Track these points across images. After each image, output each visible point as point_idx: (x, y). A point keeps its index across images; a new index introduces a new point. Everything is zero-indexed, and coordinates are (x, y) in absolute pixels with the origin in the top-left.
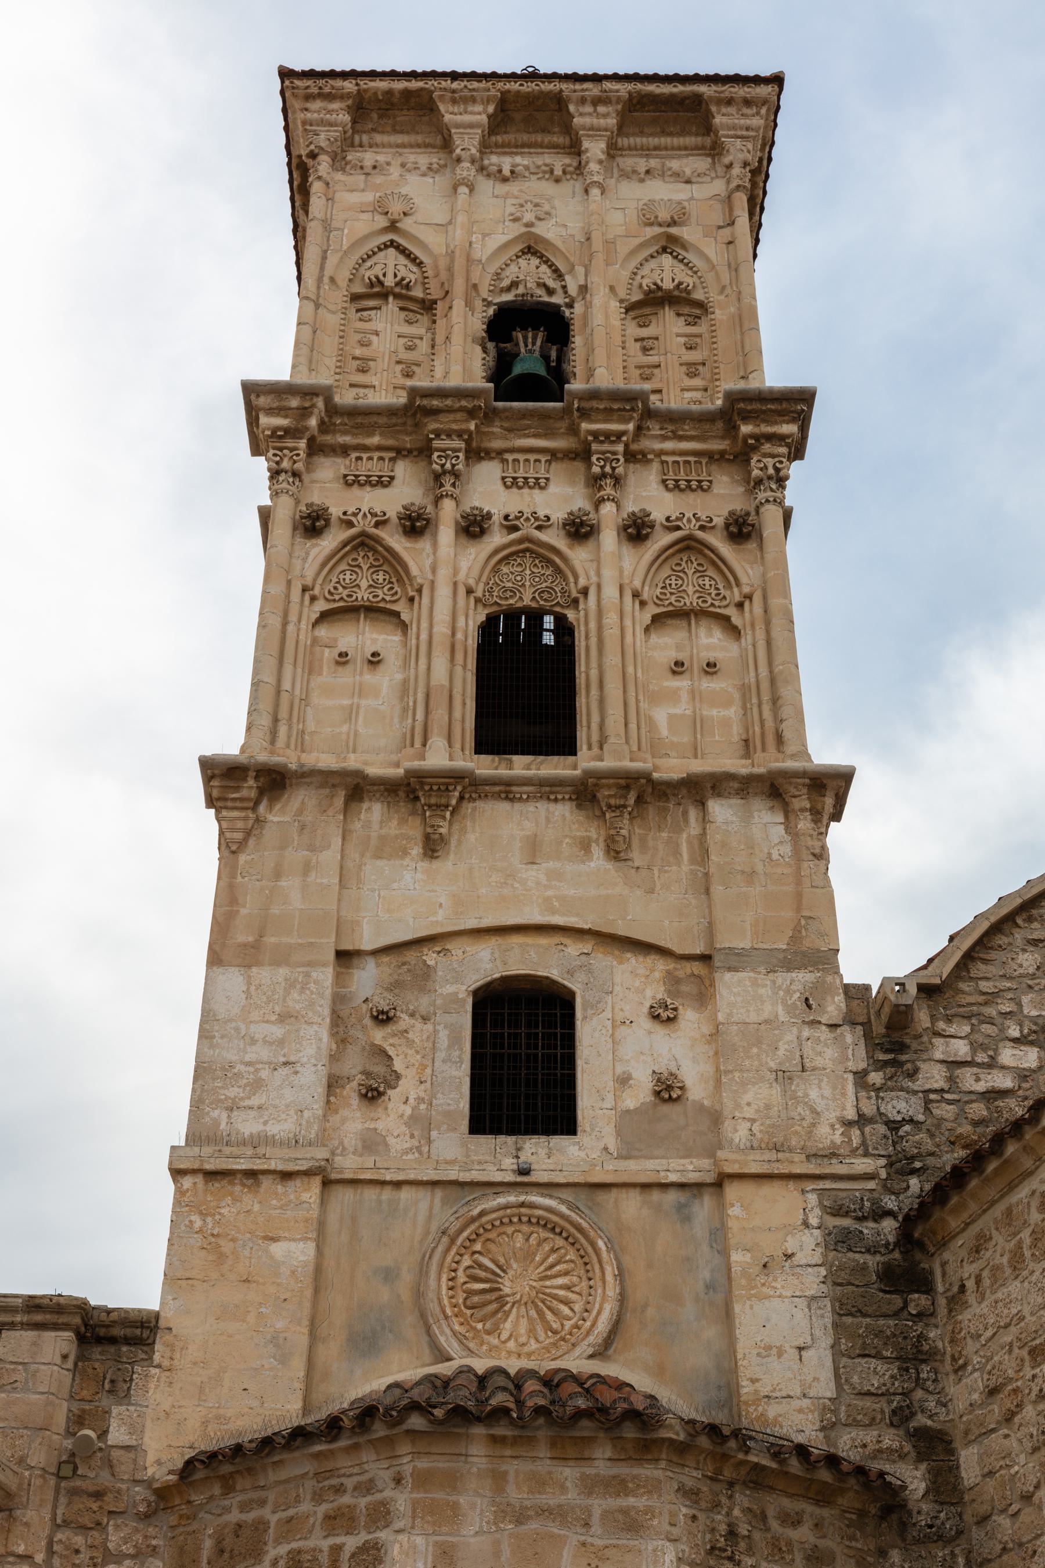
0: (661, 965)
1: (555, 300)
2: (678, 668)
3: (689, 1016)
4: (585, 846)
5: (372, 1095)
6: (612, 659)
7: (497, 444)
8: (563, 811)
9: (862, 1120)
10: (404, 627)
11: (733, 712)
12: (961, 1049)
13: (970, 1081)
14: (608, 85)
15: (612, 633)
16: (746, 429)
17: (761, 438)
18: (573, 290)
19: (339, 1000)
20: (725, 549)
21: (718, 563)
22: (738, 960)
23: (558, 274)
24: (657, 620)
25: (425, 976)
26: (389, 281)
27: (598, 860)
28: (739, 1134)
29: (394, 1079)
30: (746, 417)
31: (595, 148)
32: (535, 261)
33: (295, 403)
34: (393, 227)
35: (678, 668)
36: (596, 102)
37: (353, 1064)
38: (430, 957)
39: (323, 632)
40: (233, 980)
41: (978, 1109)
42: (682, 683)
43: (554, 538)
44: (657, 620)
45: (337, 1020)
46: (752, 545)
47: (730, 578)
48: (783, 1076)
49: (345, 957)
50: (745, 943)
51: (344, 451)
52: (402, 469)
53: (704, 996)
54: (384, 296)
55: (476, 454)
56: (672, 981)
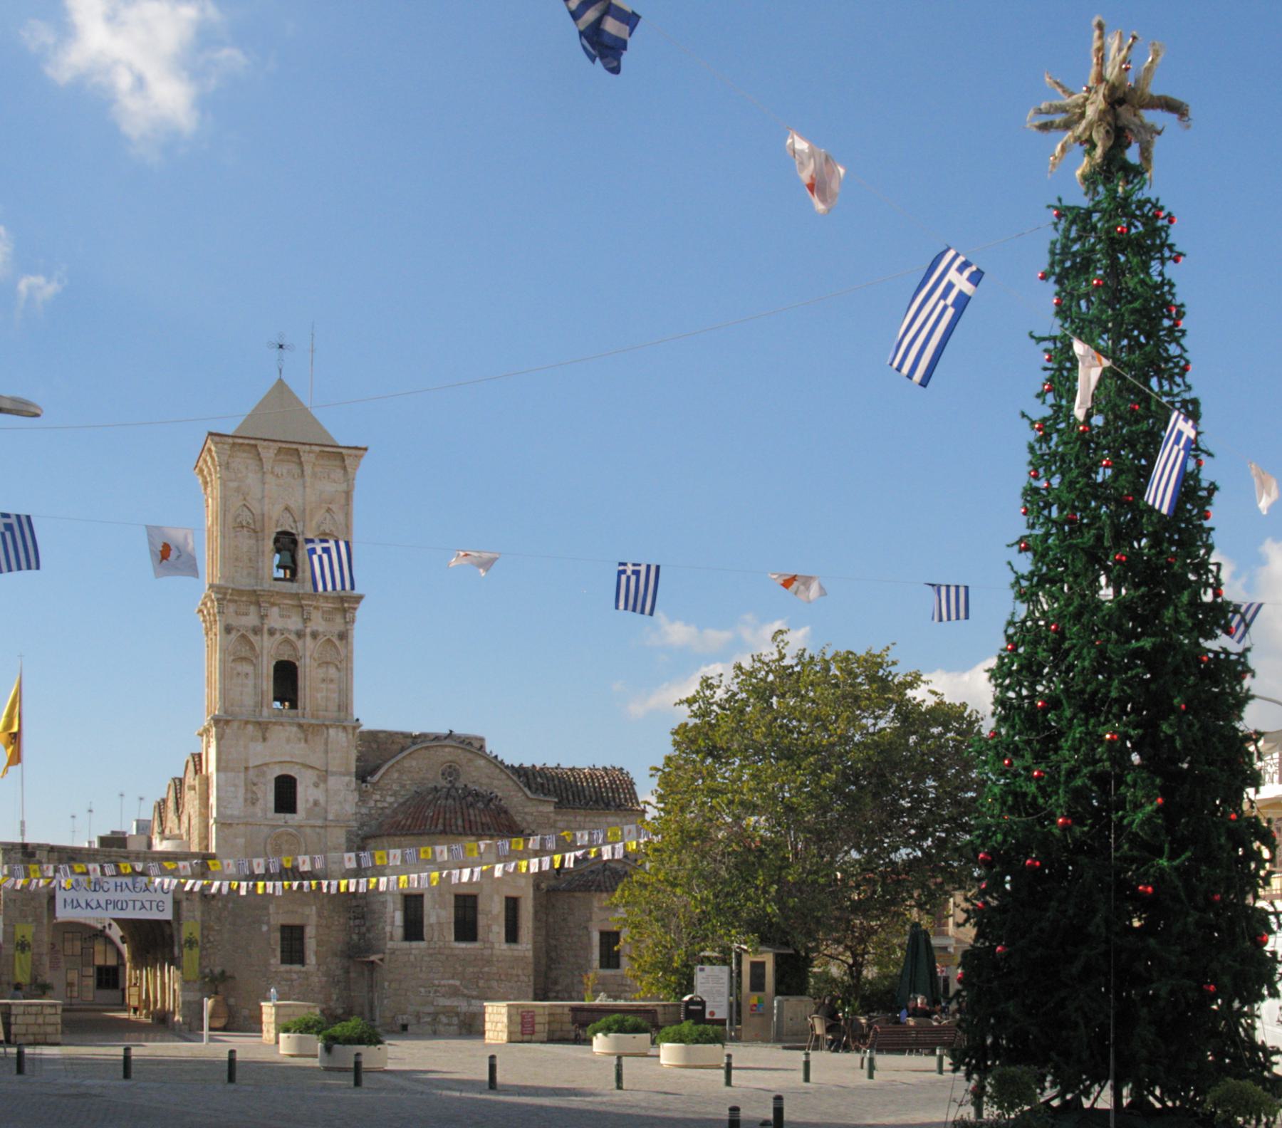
0: (317, 772)
1: (294, 531)
2: (323, 680)
3: (322, 785)
4: (300, 740)
5: (253, 804)
6: (308, 683)
7: (278, 602)
8: (295, 729)
9: (356, 814)
10: (254, 665)
11: (336, 695)
12: (378, 797)
13: (379, 805)
14: (314, 448)
15: (307, 674)
16: (346, 605)
17: (349, 608)
18: (300, 530)
19: (246, 779)
20: (337, 643)
21: (335, 646)
22: (334, 774)
23: (295, 521)
24: (319, 665)
25: (264, 773)
26: (244, 523)
27: (303, 744)
28: (331, 817)
29: (257, 800)
30: (346, 601)
31: (308, 469)
32: (288, 515)
33: (223, 590)
34: (245, 499)
35: (323, 680)
36: (309, 452)
37: (249, 795)
38: (265, 768)
39: (233, 665)
40: (222, 775)
41: (380, 812)
42: (323, 686)
43: (293, 637)
44: (319, 665)
45: (246, 785)
46: (344, 642)
47: (338, 653)
48: (340, 802)
49: (247, 768)
50: (334, 769)
51: (235, 601)
52: (253, 609)
53: (325, 781)
54: (243, 527)
55: (273, 604)
56: (319, 777)
